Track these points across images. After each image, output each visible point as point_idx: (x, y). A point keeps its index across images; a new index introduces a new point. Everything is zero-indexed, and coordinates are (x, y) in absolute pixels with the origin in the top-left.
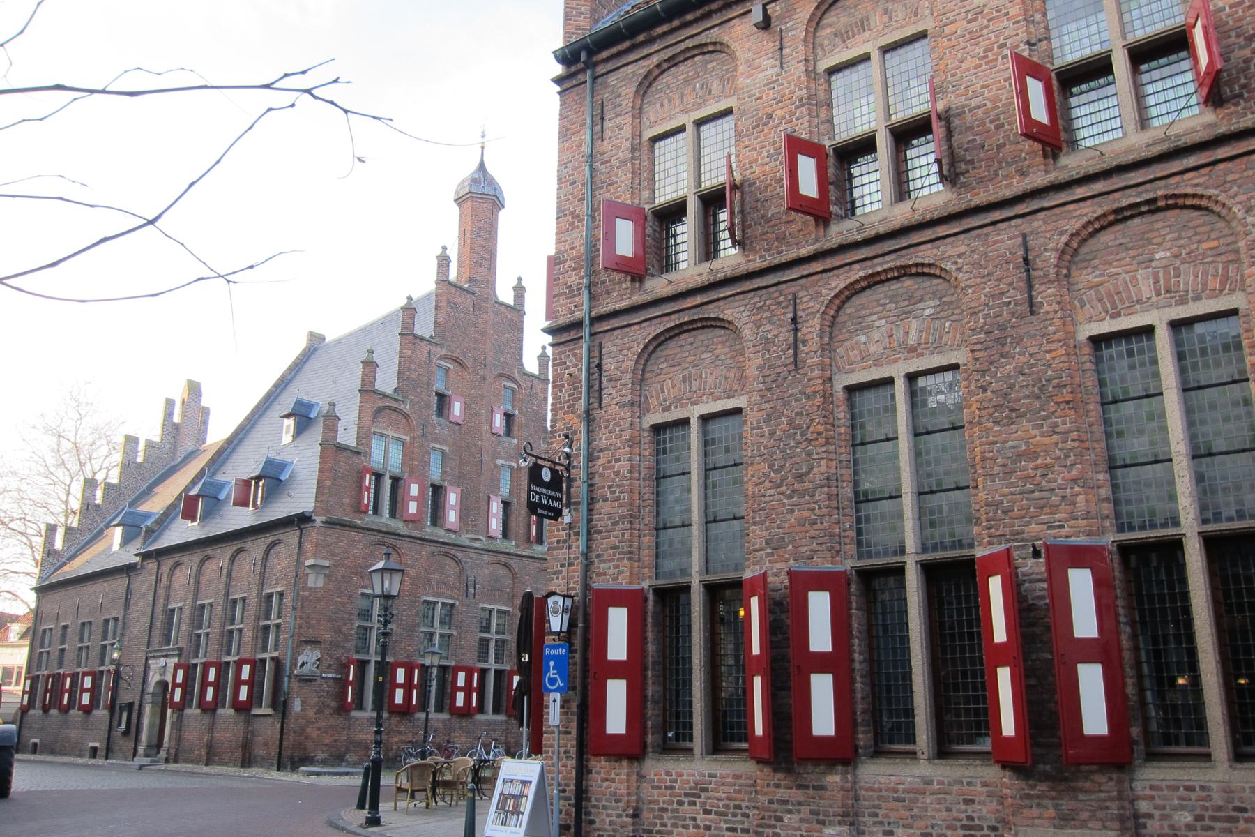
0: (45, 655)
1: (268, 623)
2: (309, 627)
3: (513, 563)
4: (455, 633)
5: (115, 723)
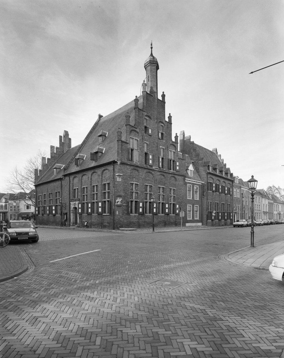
1: (94, 193)
3: (165, 174)
4: (152, 193)
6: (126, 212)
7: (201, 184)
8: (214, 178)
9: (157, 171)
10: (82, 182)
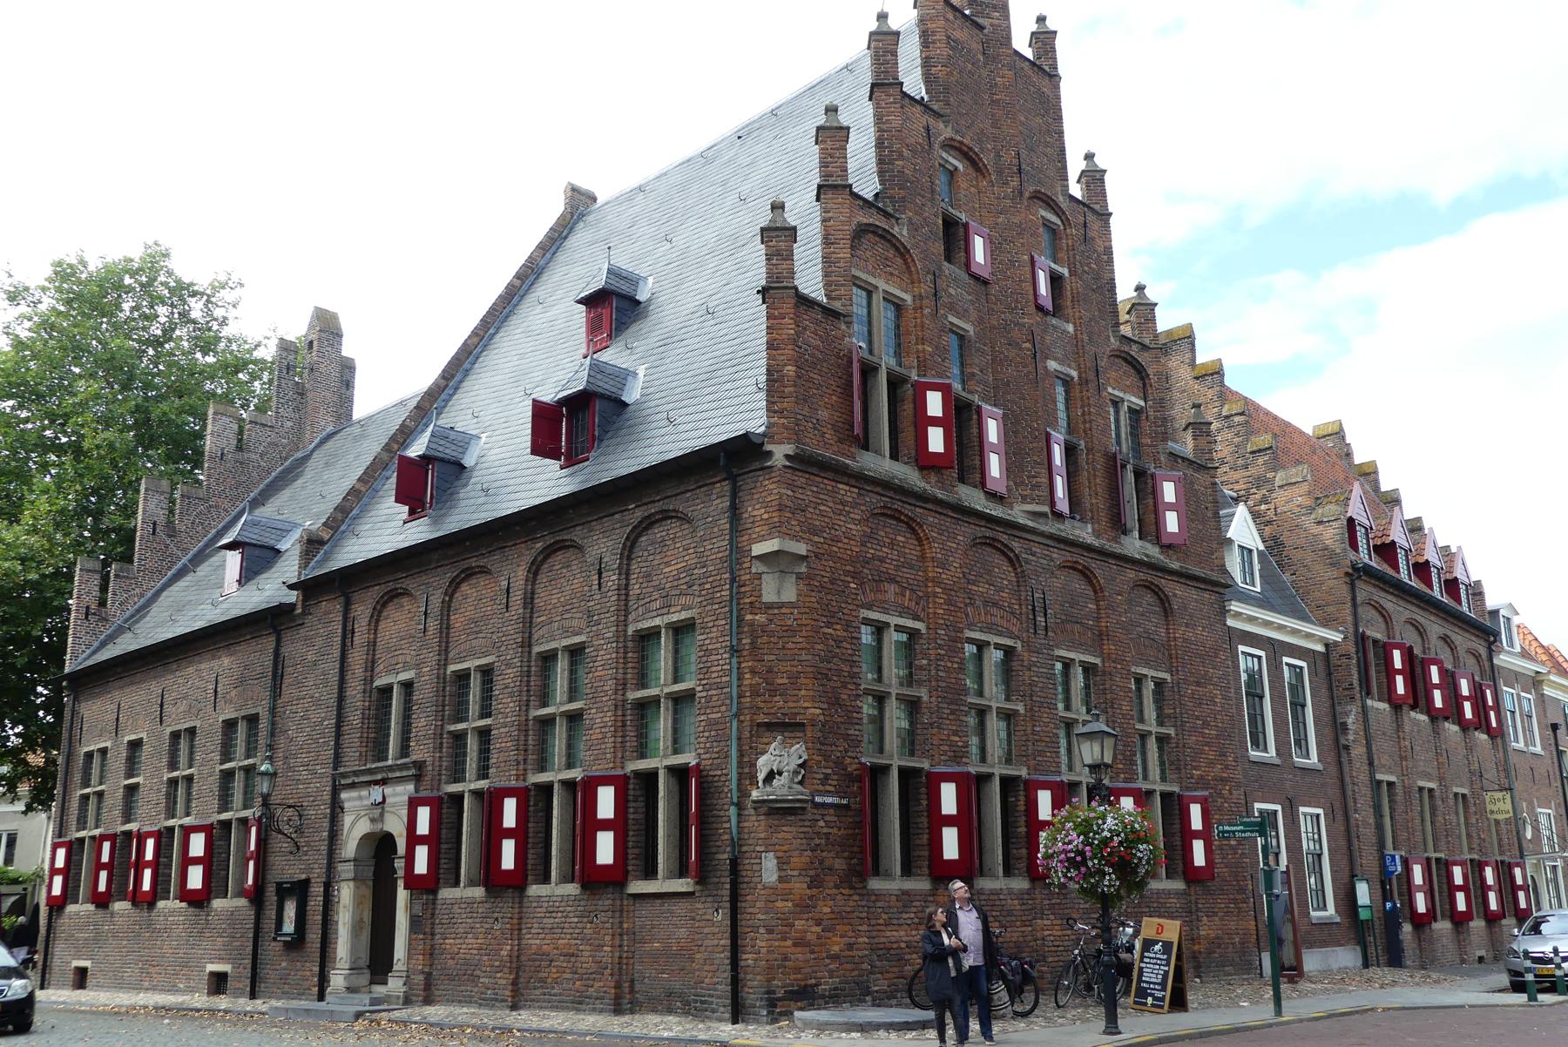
0: (93, 801)
2: (773, 693)
3: (1099, 569)
4: (1020, 708)
5: (269, 924)
6: (839, 864)
8: (1389, 606)
9: (1042, 534)
10: (445, 629)
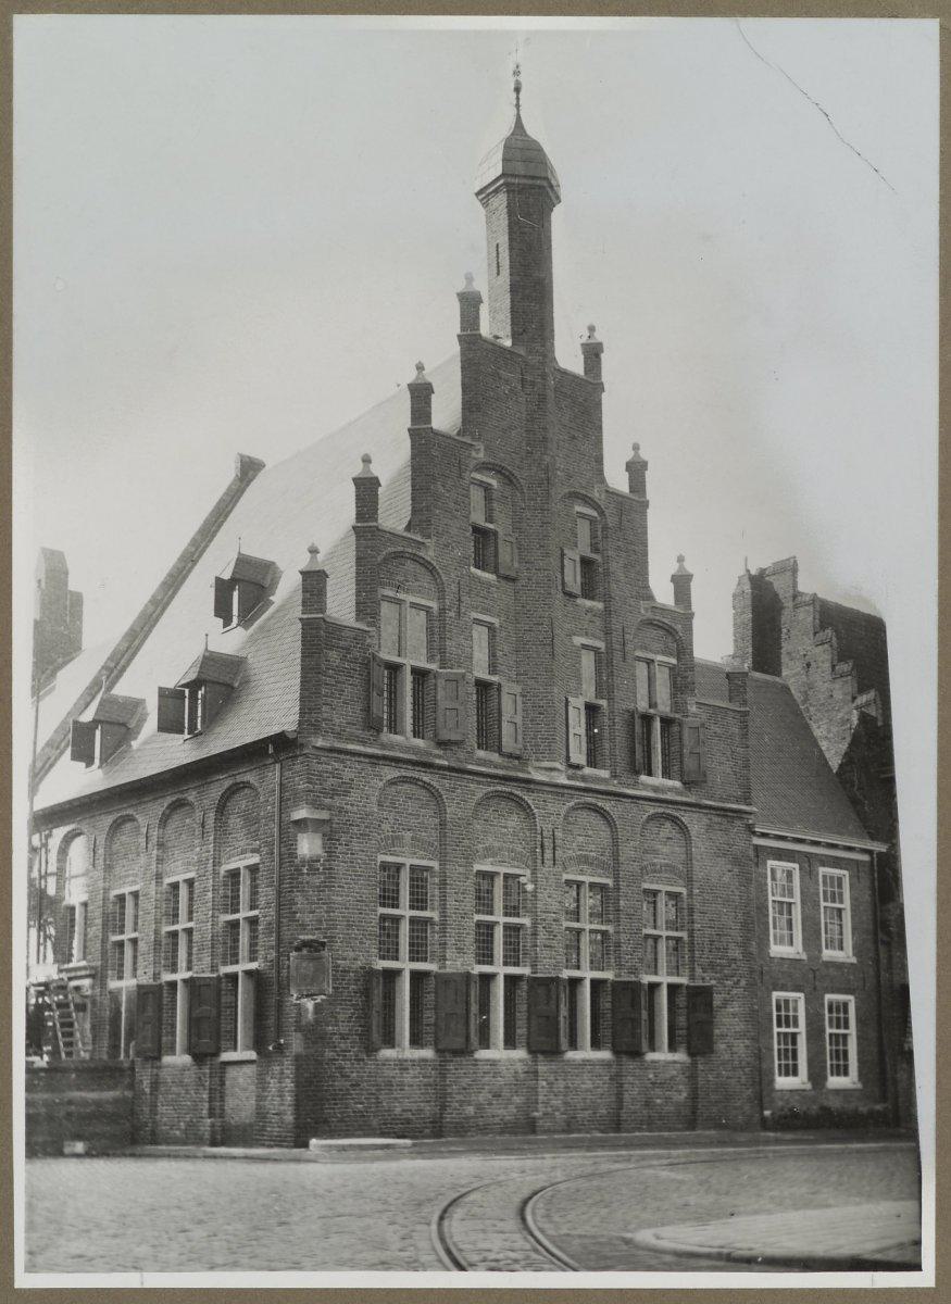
7: (866, 858)
